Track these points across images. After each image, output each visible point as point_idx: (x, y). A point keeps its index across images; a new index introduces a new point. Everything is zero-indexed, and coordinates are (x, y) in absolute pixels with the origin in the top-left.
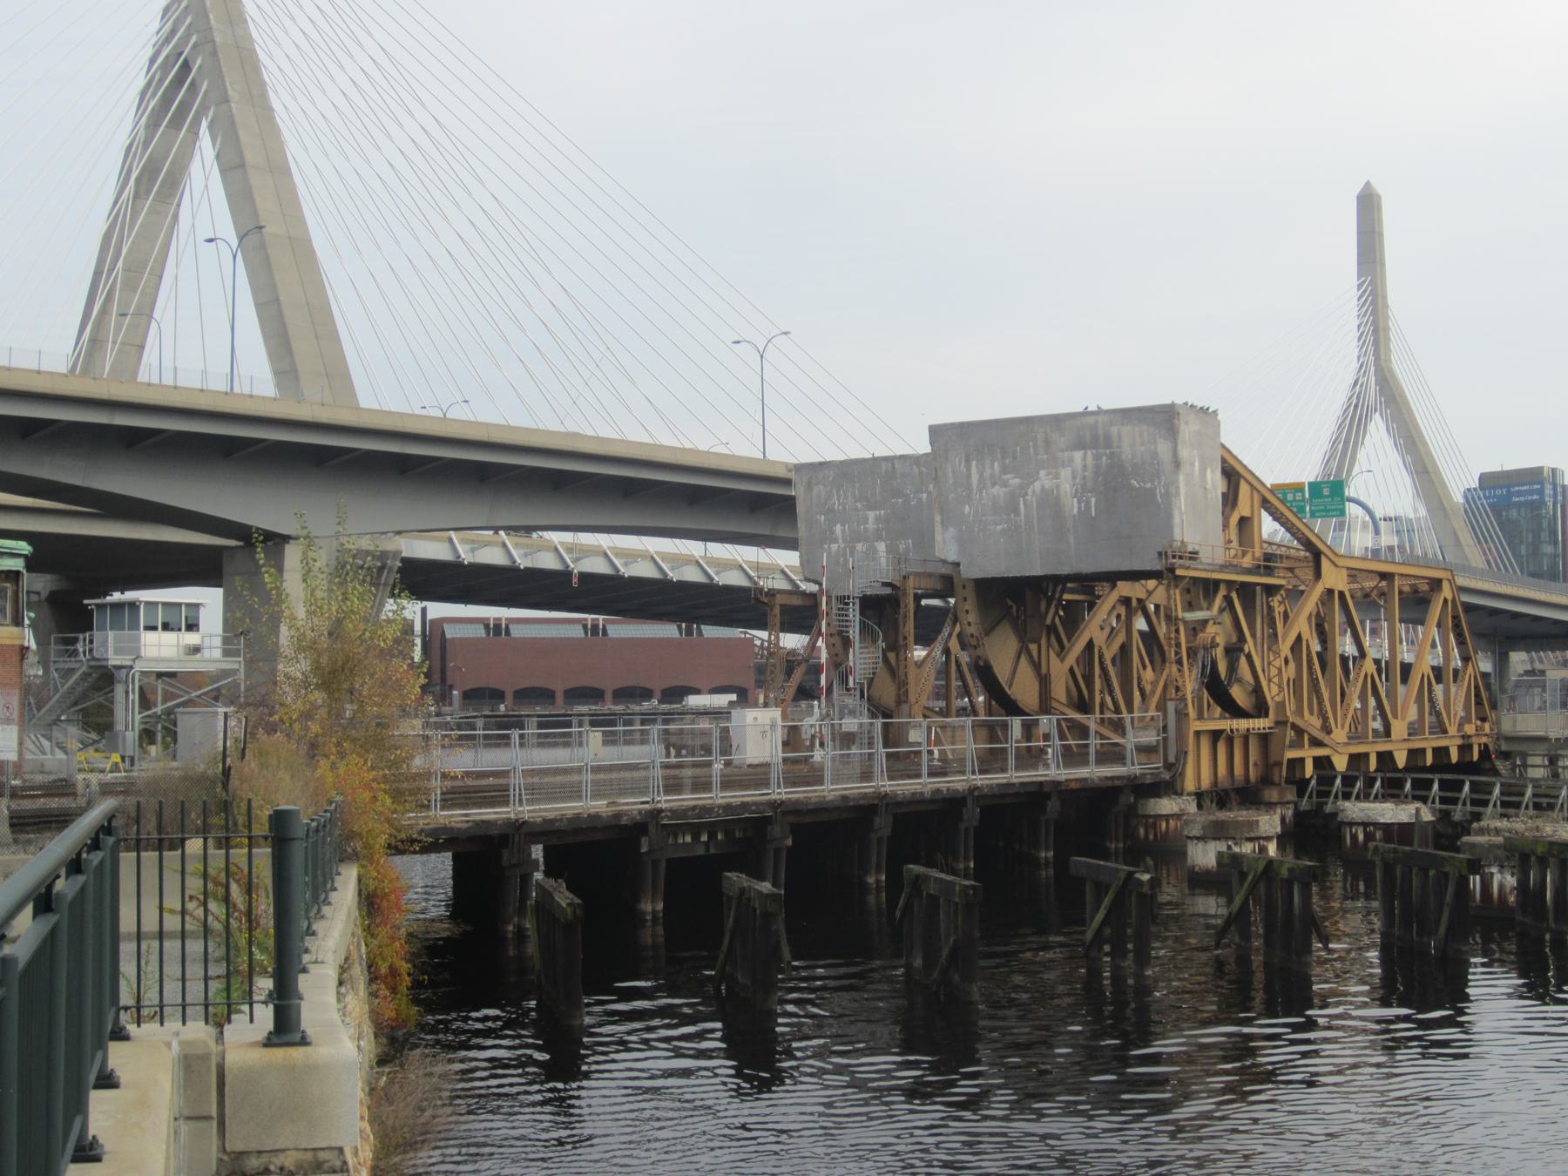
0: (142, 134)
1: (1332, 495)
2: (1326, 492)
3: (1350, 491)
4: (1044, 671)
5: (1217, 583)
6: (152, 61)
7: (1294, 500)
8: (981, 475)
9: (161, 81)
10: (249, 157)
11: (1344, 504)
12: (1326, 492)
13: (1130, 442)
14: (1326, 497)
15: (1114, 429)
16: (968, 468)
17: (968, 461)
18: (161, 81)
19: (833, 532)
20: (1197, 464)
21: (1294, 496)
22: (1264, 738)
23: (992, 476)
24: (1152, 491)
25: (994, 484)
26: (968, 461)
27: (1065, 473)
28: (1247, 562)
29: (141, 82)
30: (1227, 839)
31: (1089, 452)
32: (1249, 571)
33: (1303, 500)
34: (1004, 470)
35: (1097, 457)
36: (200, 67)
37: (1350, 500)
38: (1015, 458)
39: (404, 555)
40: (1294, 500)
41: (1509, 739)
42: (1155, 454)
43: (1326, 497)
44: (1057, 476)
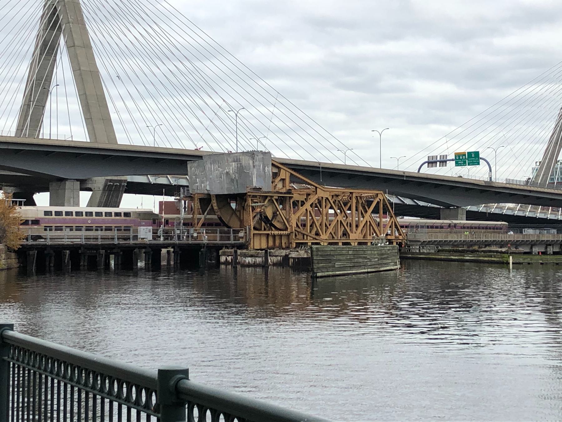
0: (42, 33)
1: (475, 157)
2: (473, 156)
3: (480, 156)
4: (242, 218)
5: (266, 197)
6: (45, 6)
7: (463, 159)
8: (214, 168)
9: (47, 14)
10: (76, 43)
11: (479, 160)
12: (473, 156)
13: (246, 161)
14: (473, 157)
15: (241, 157)
16: (211, 166)
17: (211, 165)
18: (47, 14)
19: (196, 181)
20: (261, 166)
21: (462, 157)
22: (288, 236)
23: (216, 168)
24: (249, 173)
25: (216, 171)
26: (211, 165)
27: (231, 168)
28: (284, 190)
29: (41, 13)
30: (225, 255)
31: (236, 163)
32: (285, 193)
33: (465, 159)
34: (219, 167)
35: (237, 164)
36: (60, 10)
37: (481, 158)
38: (221, 164)
39: (128, 181)
40: (463, 159)
41: (410, 241)
42: (249, 164)
43: (473, 157)
44: (229, 169)
